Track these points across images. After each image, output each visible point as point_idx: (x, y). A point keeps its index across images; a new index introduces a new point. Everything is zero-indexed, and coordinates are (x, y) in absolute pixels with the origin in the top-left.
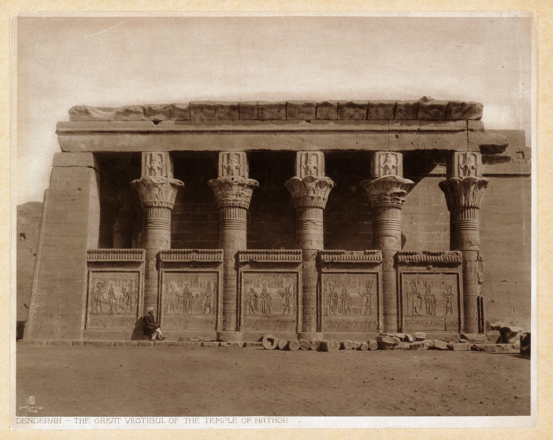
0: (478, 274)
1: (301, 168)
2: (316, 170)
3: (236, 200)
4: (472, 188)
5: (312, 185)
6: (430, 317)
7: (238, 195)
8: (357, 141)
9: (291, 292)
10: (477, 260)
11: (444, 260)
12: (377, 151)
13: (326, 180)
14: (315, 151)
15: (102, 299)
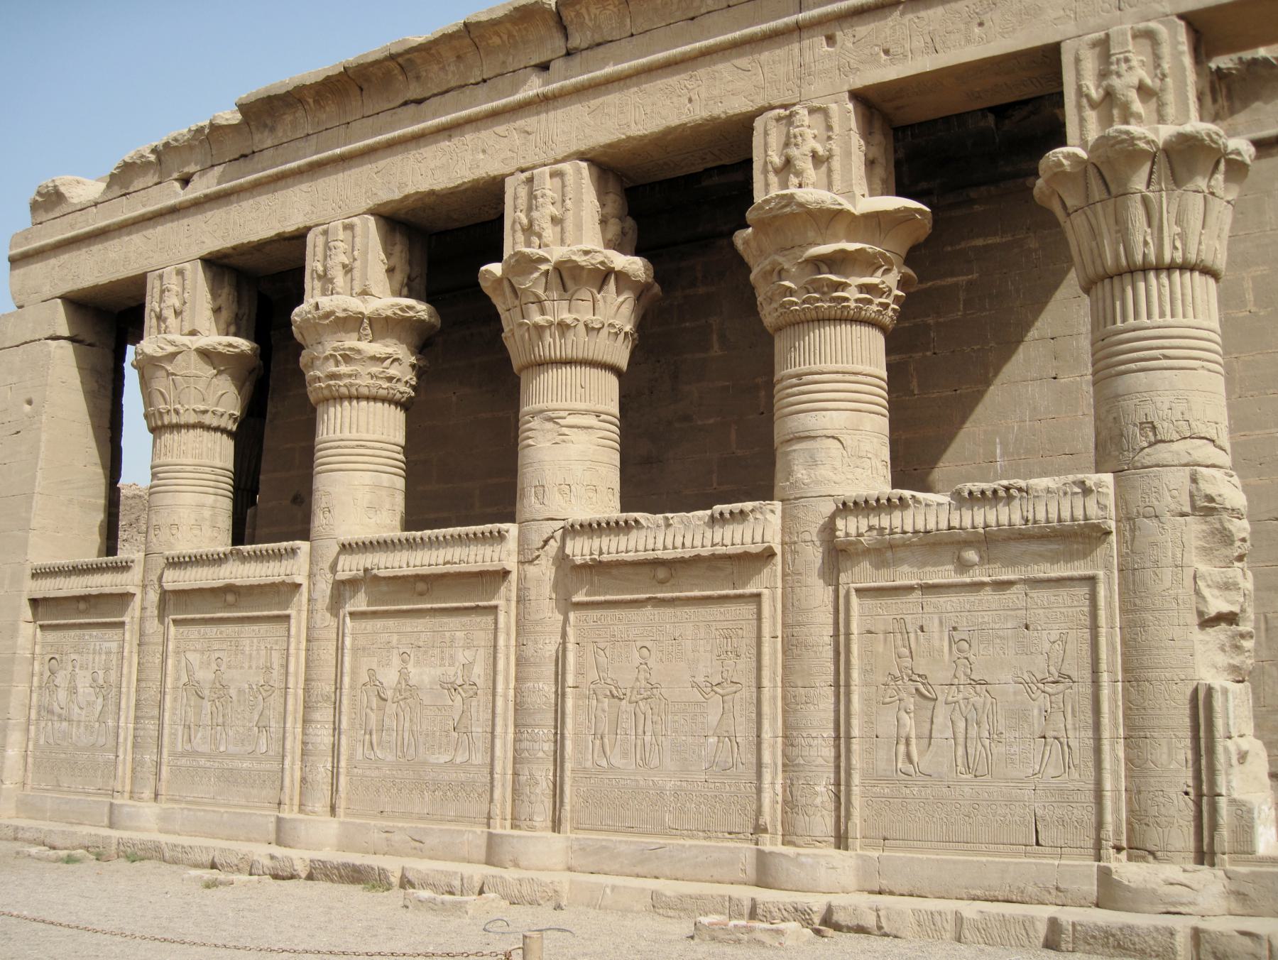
0: (1195, 578)
1: (514, 231)
2: (558, 229)
3: (333, 376)
4: (1139, 183)
5: (532, 283)
6: (966, 781)
7: (339, 357)
8: (692, 94)
10: (1187, 509)
11: (1027, 521)
12: (761, 111)
13: (574, 258)
14: (557, 162)
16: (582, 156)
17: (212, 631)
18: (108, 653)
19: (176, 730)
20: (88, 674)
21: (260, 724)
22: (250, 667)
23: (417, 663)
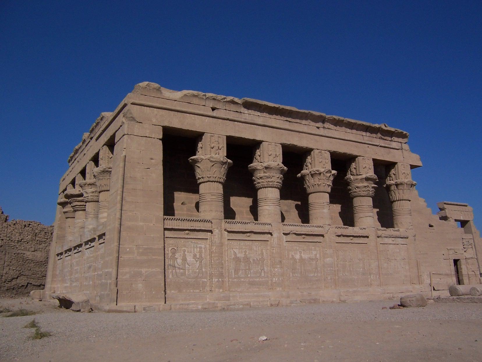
9: (318, 258)
16: (329, 151)
17: (242, 243)
18: (201, 248)
19: (232, 271)
20: (192, 255)
22: (256, 254)
23: (304, 254)
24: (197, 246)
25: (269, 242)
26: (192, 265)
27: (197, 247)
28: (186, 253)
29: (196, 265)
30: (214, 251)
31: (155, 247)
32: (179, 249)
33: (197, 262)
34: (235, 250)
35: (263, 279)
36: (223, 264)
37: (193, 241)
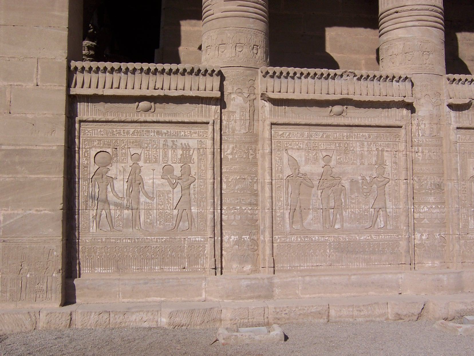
15: (111, 196)
18: (186, 148)
19: (283, 214)
21: (376, 206)
22: (362, 164)
24: (173, 144)
25: (403, 131)
26: (159, 196)
27: (174, 148)
28: (141, 163)
29: (171, 195)
30: (230, 157)
31: (38, 148)
32: (120, 152)
33: (174, 189)
34: (295, 155)
35: (382, 237)
36: (256, 195)
37: (164, 129)
